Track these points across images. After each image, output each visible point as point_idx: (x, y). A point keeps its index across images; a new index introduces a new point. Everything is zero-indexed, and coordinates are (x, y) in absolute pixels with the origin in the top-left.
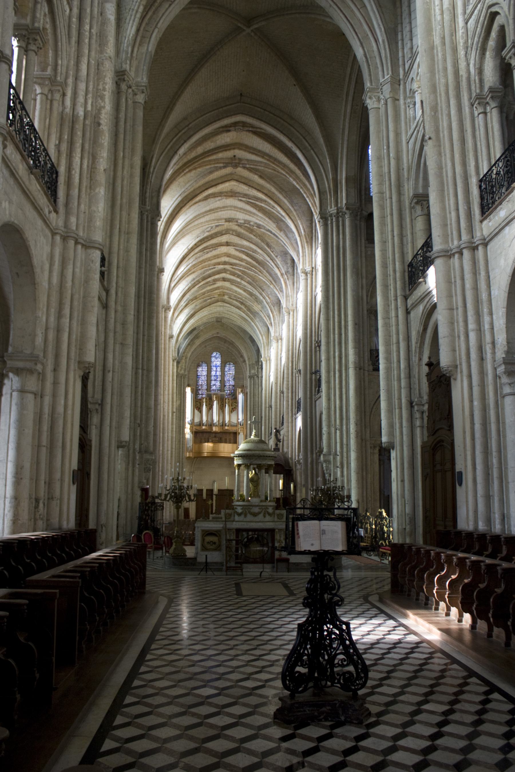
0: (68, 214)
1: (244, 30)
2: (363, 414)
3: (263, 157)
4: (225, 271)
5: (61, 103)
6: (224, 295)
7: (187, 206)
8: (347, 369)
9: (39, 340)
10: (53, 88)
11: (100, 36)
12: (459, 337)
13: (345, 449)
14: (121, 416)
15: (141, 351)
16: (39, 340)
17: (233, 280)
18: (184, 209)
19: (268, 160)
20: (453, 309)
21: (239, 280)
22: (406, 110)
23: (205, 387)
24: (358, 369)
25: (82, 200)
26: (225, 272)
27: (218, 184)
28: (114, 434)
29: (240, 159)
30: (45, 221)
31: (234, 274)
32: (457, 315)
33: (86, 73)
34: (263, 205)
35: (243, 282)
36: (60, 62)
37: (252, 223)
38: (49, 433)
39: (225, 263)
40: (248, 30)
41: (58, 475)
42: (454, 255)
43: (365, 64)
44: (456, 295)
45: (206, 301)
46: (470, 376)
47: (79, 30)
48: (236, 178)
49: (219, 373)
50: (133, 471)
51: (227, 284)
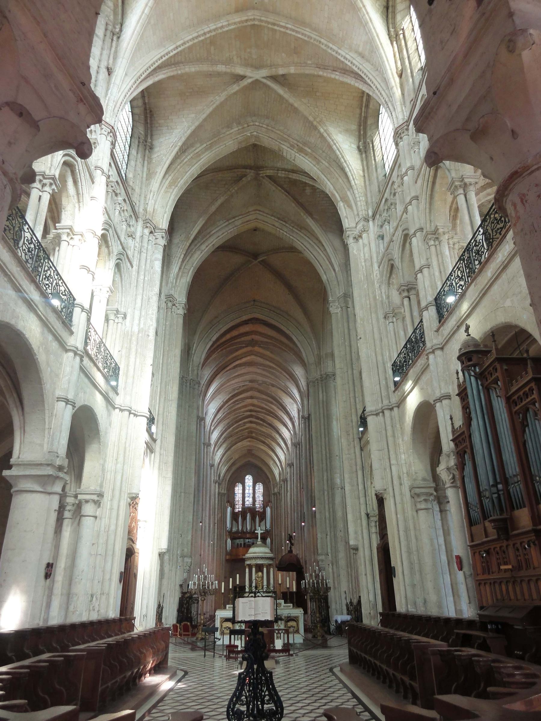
4: (251, 416)
6: (252, 433)
10: (118, 316)
21: (262, 423)
23: (241, 502)
27: (243, 358)
31: (258, 418)
35: (265, 424)
39: (251, 411)
40: (256, 262)
49: (251, 491)
51: (254, 425)
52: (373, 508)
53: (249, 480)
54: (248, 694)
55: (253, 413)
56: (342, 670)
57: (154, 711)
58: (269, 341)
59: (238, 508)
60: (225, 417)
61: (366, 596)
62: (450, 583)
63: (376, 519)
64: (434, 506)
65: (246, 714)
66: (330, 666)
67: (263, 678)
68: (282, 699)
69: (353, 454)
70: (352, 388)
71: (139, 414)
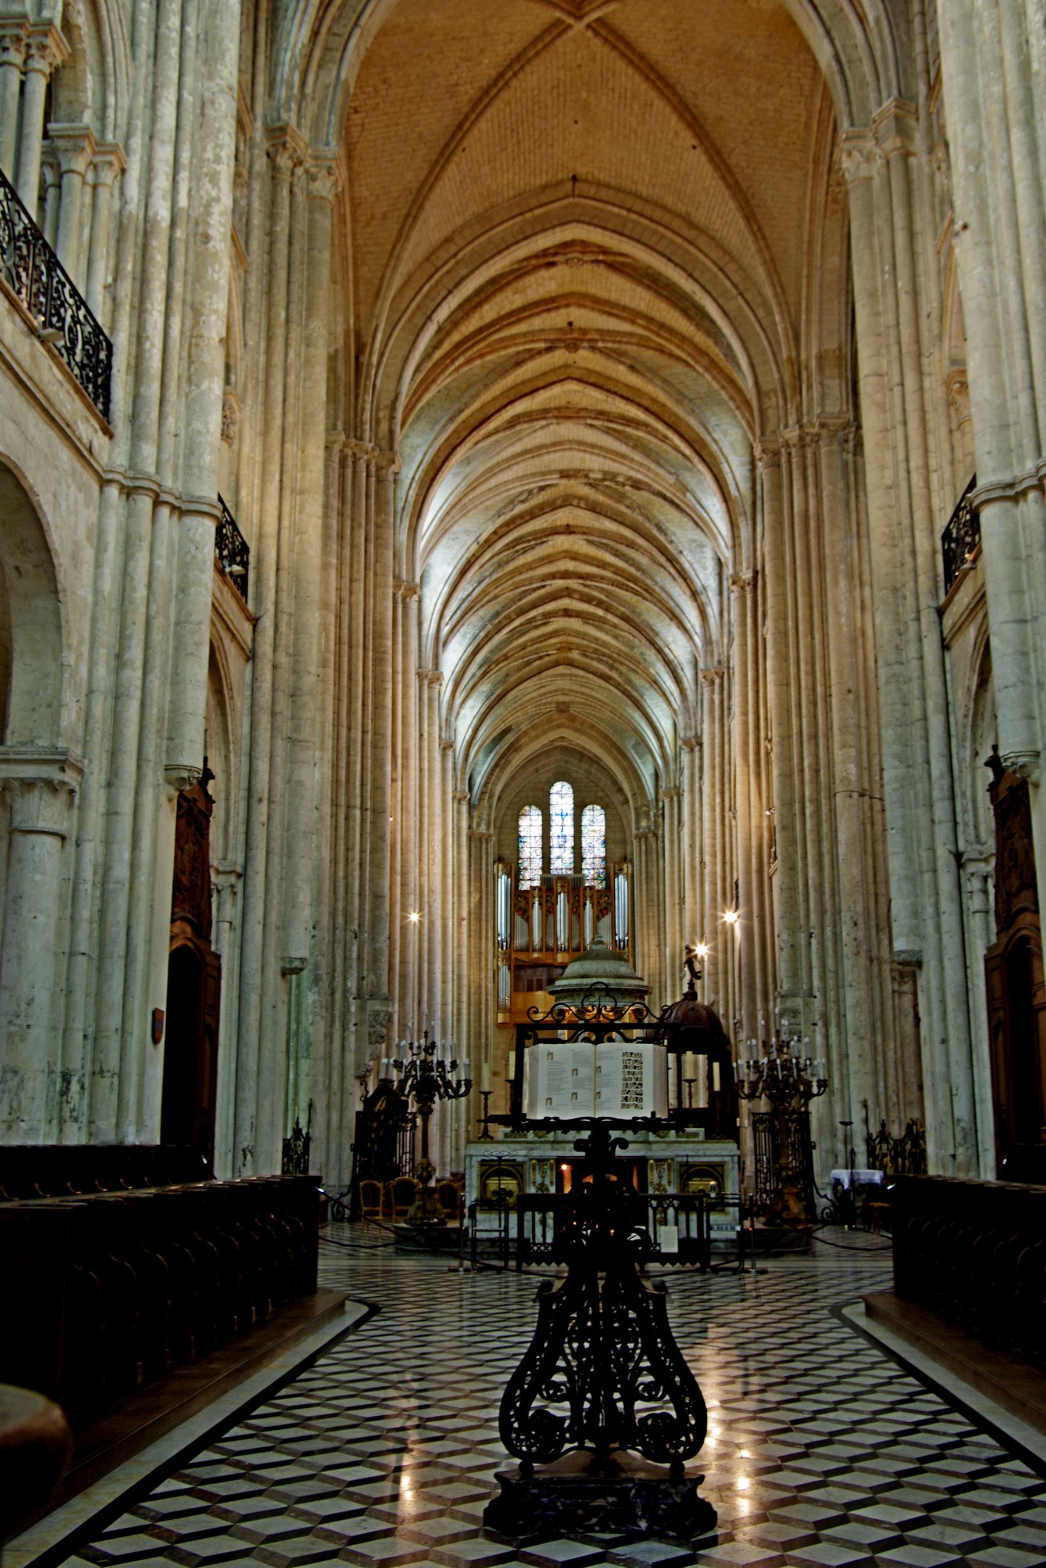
0: (136, 436)
1: (569, 27)
3: (633, 322)
4: (568, 593)
5: (116, 192)
11: (206, 40)
13: (831, 983)
14: (290, 901)
15: (359, 767)
16: (70, 716)
19: (645, 328)
21: (600, 612)
22: (932, 177)
23: (538, 863)
24: (855, 795)
25: (168, 408)
26: (570, 596)
27: (537, 390)
28: (272, 942)
29: (584, 331)
30: (83, 454)
31: (588, 599)
33: (172, 124)
34: (641, 434)
35: (610, 617)
36: (111, 100)
37: (620, 479)
38: (95, 925)
39: (565, 575)
40: (579, 26)
41: (114, 1021)
42: (1024, 493)
43: (838, 78)
47: (157, 27)
48: (577, 374)
49: (569, 831)
50: (343, 1039)
51: (575, 624)
55: (573, 584)
56: (870, 1311)
57: (262, 1410)
58: (625, 327)
59: (532, 877)
60: (485, 592)
63: (990, 867)
65: (569, 1429)
66: (831, 1301)
67: (632, 1315)
69: (914, 664)
70: (915, 439)
71: (185, 507)
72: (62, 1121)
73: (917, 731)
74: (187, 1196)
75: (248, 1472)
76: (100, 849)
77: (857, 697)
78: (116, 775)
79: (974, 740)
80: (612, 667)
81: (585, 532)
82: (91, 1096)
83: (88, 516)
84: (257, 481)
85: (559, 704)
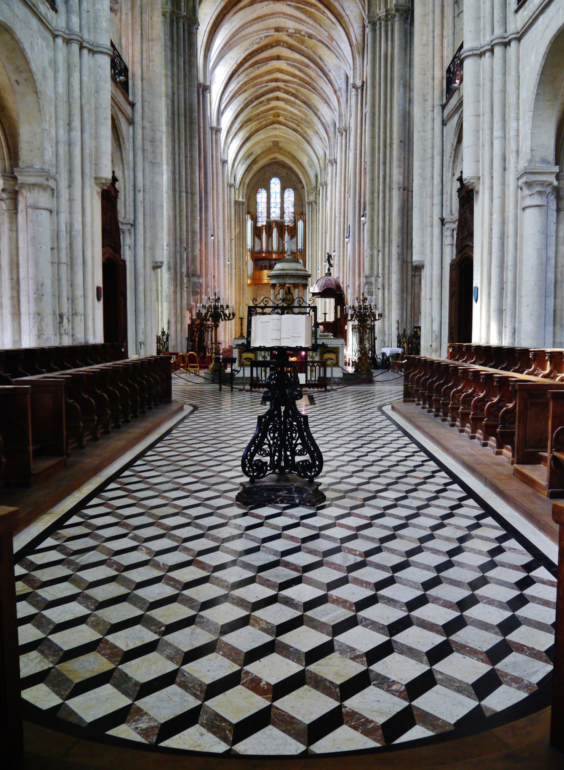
2: (405, 236)
4: (278, 89)
6: (279, 116)
7: (231, 13)
8: (391, 189)
9: (49, 154)
12: (483, 145)
13: (386, 271)
16: (49, 154)
17: (287, 99)
18: (228, 17)
20: (479, 116)
23: (265, 214)
24: (401, 189)
31: (287, 92)
32: (483, 122)
34: (313, 10)
35: (297, 101)
37: (303, 33)
38: (68, 250)
39: (277, 80)
44: (483, 99)
45: (260, 123)
46: (492, 188)
49: (279, 200)
50: (181, 294)
51: (281, 104)
52: (451, 211)
53: (275, 184)
54: (271, 442)
55: (281, 84)
56: (393, 408)
57: (150, 453)
59: (262, 222)
61: (428, 325)
62: (552, 308)
63: (455, 225)
64: (550, 203)
65: (270, 466)
66: (378, 404)
67: (295, 423)
68: (322, 450)
69: (430, 132)
71: (95, 49)
72: (61, 335)
73: (429, 163)
74: (115, 369)
75: (143, 480)
76: (68, 216)
77: (405, 144)
78: (72, 182)
79: (453, 168)
80: (298, 125)
81: (287, 59)
82: (73, 324)
83: (48, 54)
84: (130, 34)
85: (274, 142)
